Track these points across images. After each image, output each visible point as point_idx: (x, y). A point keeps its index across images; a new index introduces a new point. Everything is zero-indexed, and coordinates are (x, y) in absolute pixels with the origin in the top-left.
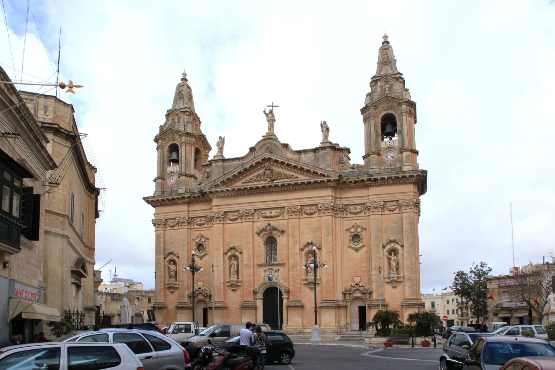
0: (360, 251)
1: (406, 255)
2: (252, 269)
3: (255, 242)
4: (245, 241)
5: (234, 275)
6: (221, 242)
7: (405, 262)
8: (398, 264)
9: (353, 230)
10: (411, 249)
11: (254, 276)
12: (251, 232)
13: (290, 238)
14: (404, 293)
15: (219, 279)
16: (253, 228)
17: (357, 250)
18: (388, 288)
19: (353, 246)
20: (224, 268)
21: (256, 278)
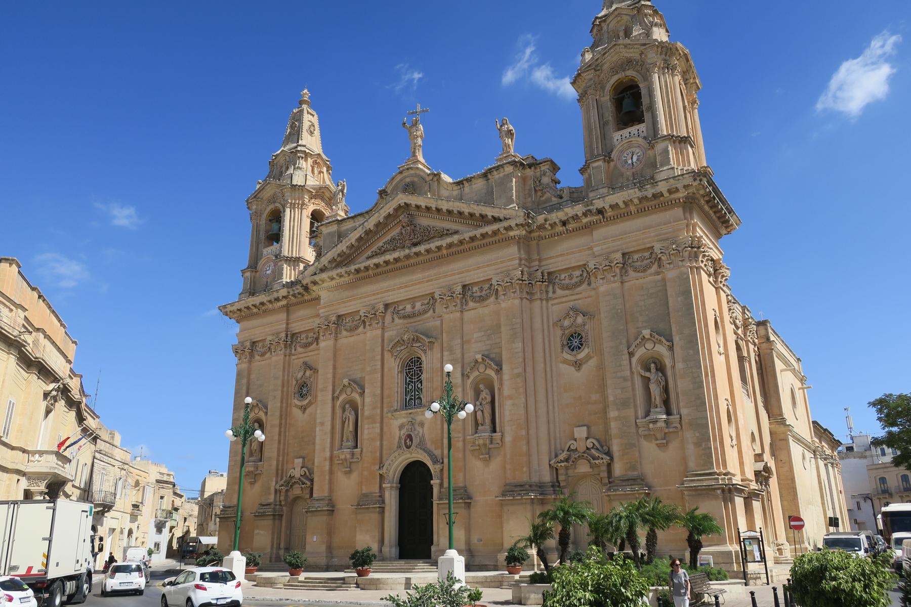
0: (584, 368)
1: (680, 366)
2: (378, 425)
3: (386, 370)
4: (368, 369)
5: (348, 440)
6: (330, 376)
7: (679, 382)
8: (666, 390)
9: (566, 323)
10: (691, 352)
11: (381, 440)
12: (380, 348)
13: (445, 353)
14: (684, 460)
15: (324, 450)
16: (383, 340)
17: (578, 365)
18: (649, 448)
19: (569, 357)
20: (333, 427)
21: (385, 443)
